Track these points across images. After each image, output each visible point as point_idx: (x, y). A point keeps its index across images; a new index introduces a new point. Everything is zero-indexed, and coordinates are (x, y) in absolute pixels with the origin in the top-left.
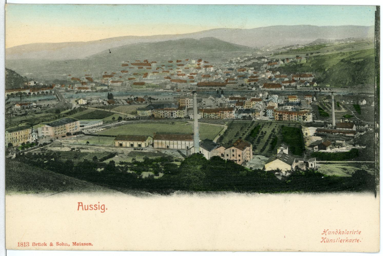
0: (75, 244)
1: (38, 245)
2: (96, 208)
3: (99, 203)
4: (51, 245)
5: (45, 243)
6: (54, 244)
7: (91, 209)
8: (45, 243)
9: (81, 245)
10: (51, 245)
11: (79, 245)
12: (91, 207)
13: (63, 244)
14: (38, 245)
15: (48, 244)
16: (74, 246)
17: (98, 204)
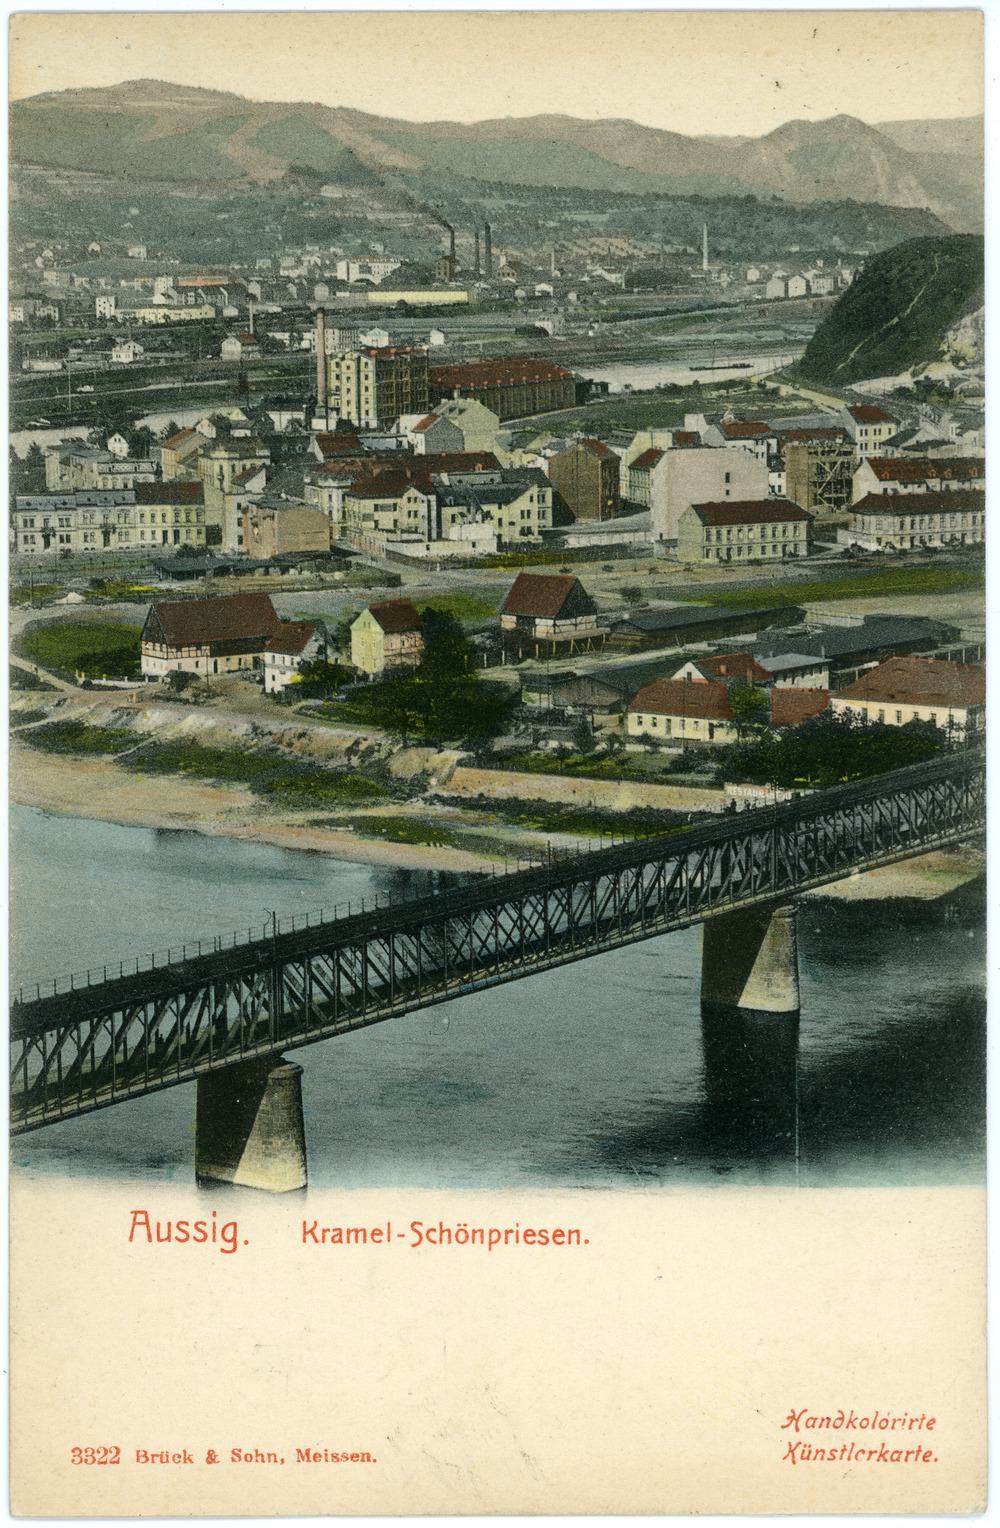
0: (305, 1455)
1: (157, 1459)
2: (200, 1236)
3: (214, 1214)
4: (211, 1458)
5: (185, 1452)
6: (224, 1455)
7: (182, 1236)
8: (185, 1452)
9: (330, 1457)
10: (211, 1458)
11: (323, 1458)
12: (183, 1231)
13: (258, 1456)
14: (157, 1459)
15: (200, 1456)
16: (304, 1464)
17: (209, 1221)
